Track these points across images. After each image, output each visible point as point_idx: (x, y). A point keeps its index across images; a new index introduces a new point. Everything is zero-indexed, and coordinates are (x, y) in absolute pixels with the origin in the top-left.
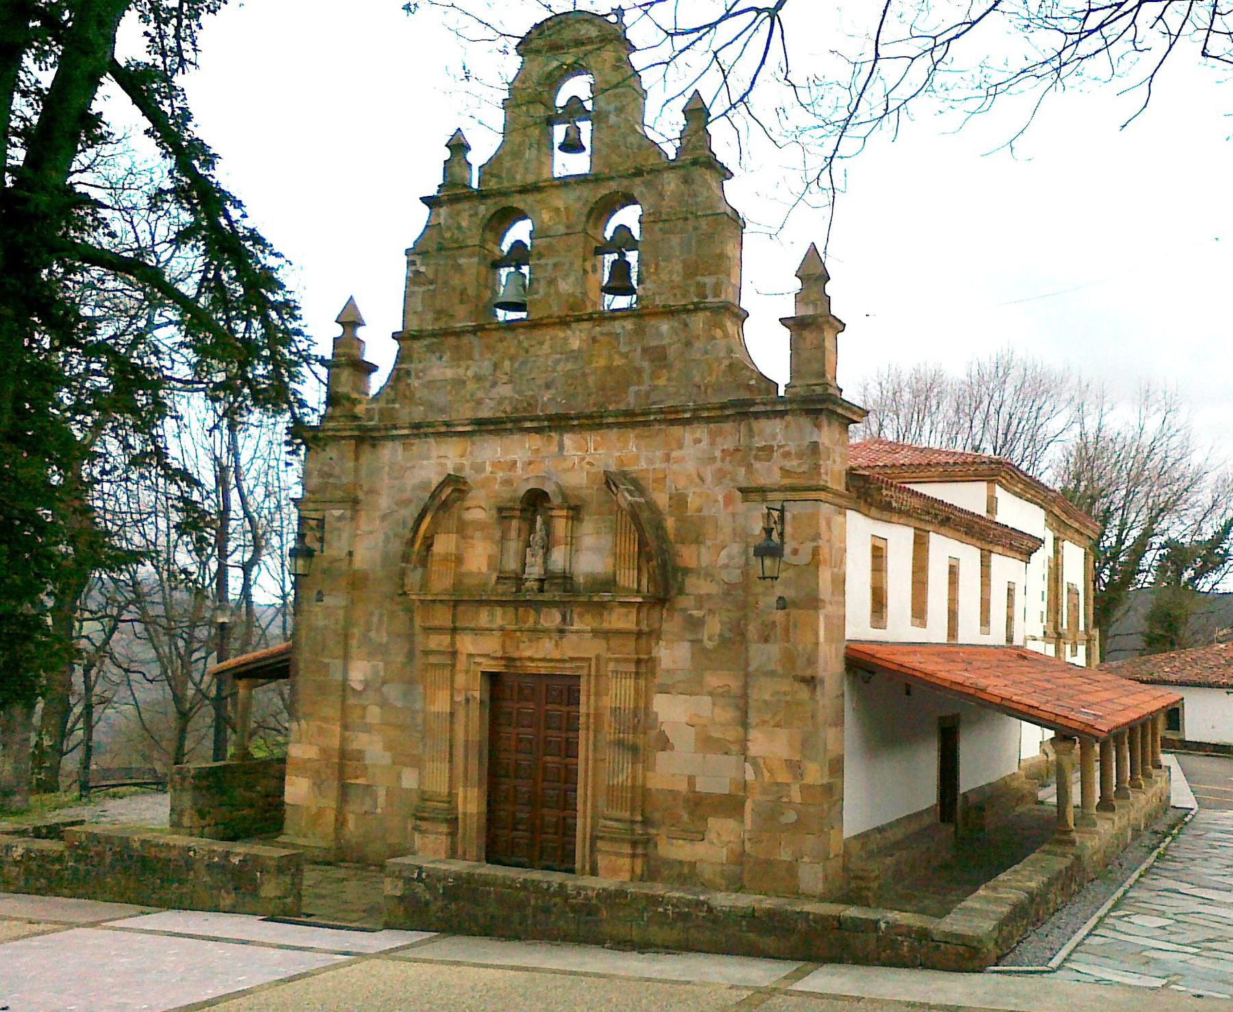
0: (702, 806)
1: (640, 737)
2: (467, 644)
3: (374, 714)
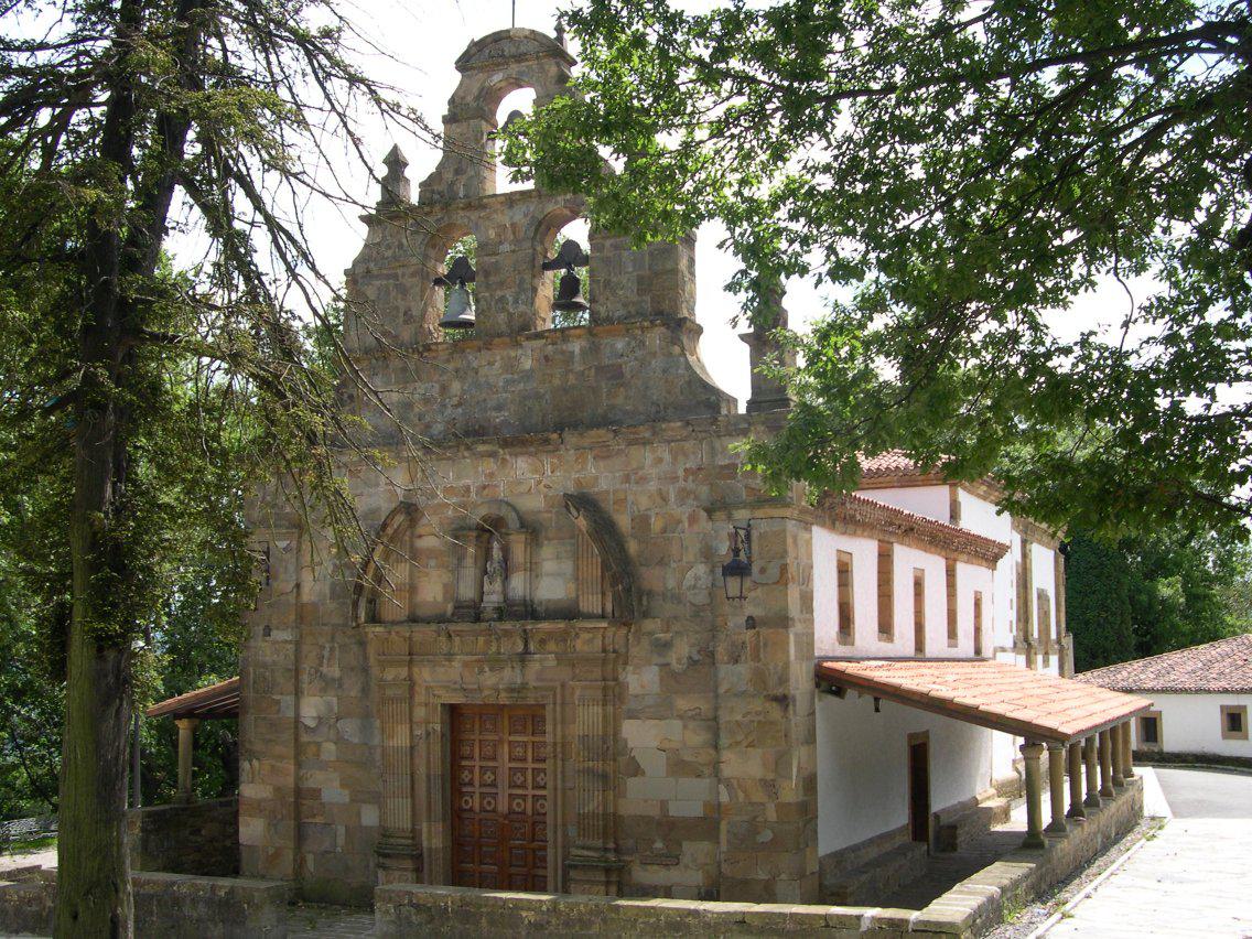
2: (424, 675)
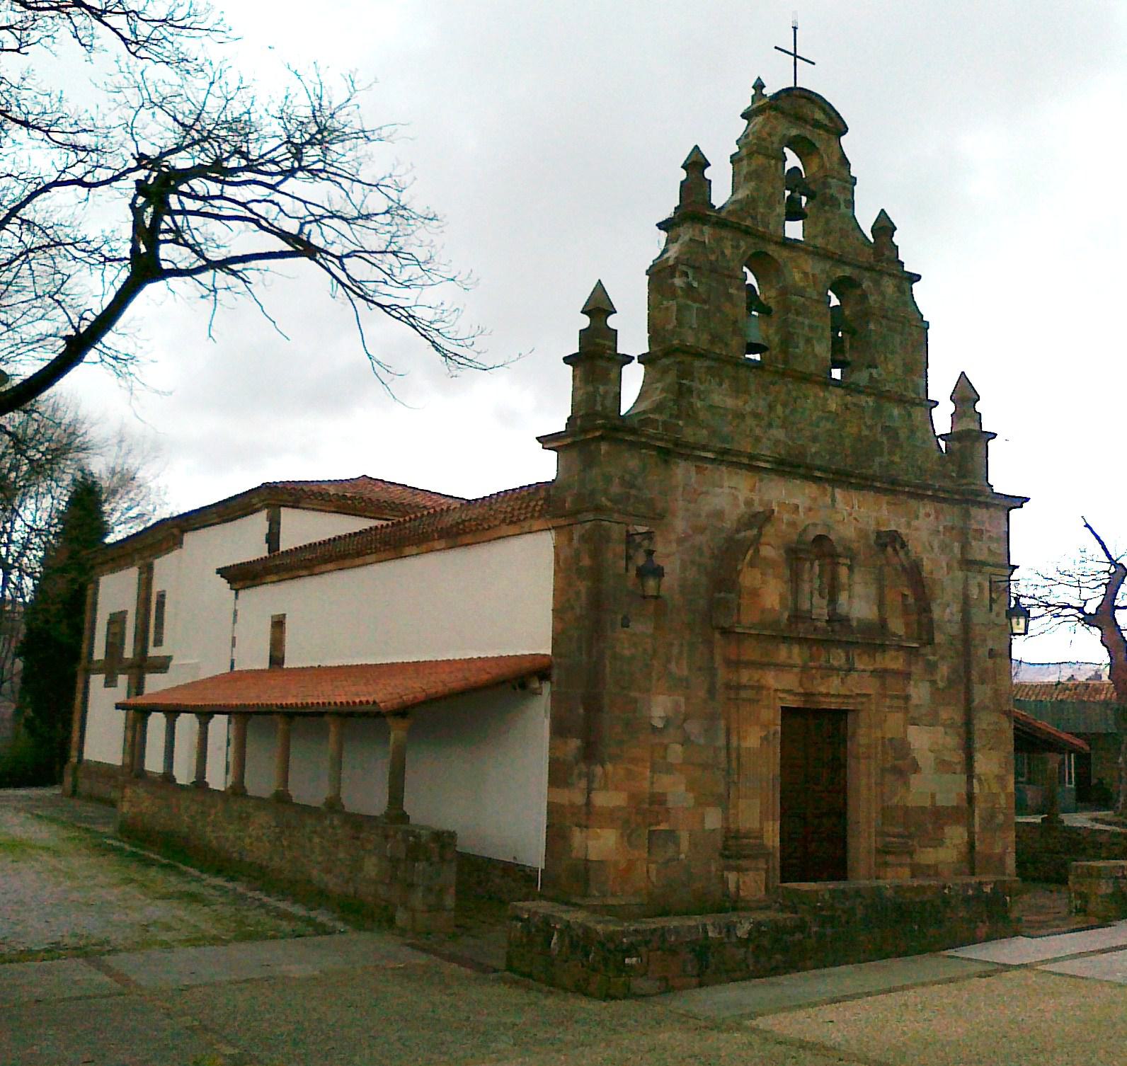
0: (940, 816)
1: (901, 764)
2: (771, 679)
3: (676, 752)
